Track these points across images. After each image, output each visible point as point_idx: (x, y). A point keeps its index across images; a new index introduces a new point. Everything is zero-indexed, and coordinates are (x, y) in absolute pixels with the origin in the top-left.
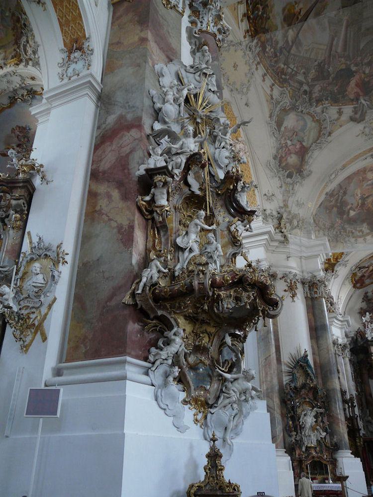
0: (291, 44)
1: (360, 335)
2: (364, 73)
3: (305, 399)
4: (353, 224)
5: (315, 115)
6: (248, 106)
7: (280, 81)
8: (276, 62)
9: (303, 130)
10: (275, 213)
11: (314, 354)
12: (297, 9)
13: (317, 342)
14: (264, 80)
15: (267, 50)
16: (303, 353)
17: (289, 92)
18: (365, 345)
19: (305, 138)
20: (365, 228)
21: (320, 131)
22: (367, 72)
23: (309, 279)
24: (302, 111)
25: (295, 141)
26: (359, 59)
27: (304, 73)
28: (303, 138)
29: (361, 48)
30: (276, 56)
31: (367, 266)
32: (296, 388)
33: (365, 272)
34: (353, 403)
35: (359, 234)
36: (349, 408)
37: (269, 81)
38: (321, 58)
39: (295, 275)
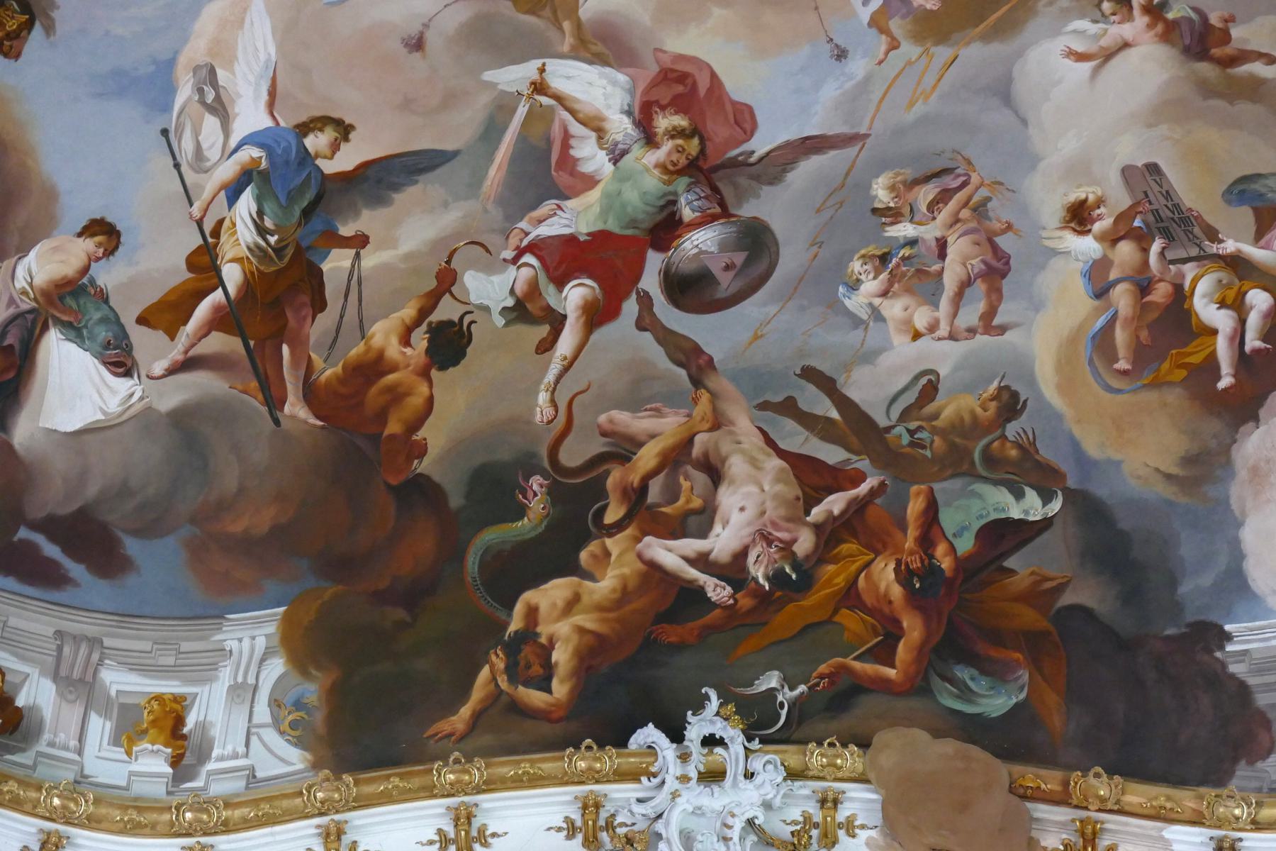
20: (243, 692)
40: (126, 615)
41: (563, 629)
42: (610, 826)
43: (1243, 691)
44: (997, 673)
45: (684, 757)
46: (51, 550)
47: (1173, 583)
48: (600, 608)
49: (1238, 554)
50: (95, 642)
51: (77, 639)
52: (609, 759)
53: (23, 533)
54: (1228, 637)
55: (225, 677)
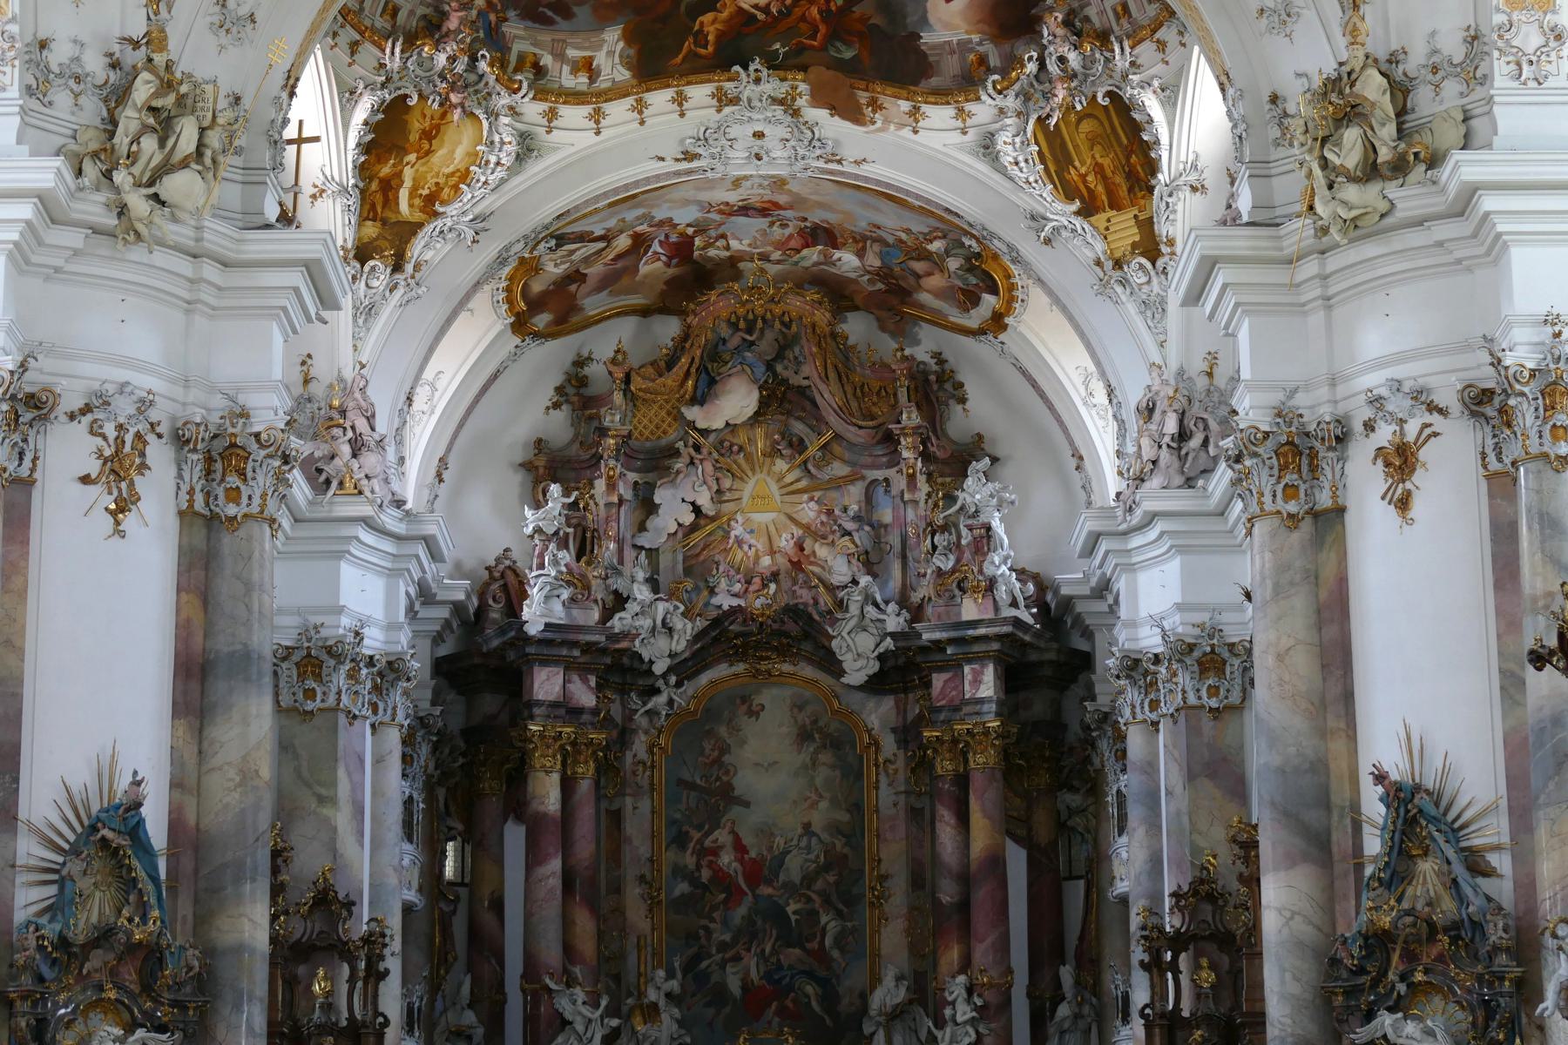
1: (505, 587)
3: (100, 988)
4: (546, 21)
10: (95, 65)
11: (176, 784)
13: (200, 733)
16: (123, 783)
18: (511, 655)
20: (611, 53)
23: (215, 419)
31: (599, 232)
32: (63, 942)
33: (586, 260)
34: (374, 959)
35: (569, 80)
36: (352, 980)
39: (144, 405)
40: (574, 32)
41: (711, 29)
42: (725, 94)
43: (925, 55)
44: (848, 44)
45: (748, 76)
46: (550, 13)
47: (905, 17)
48: (724, 22)
49: (925, 12)
50: (564, 41)
51: (559, 41)
52: (727, 75)
53: (541, 9)
54: (921, 37)
55: (605, 49)
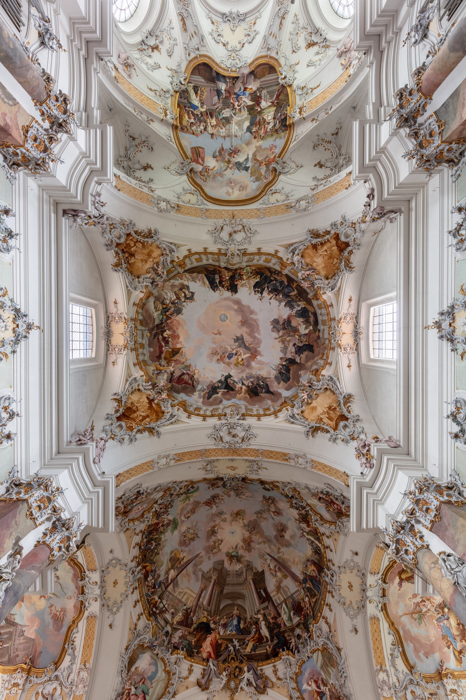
0: (170, 581)
2: (219, 634)
5: (168, 664)
6: (111, 628)
7: (149, 612)
8: (153, 593)
9: (151, 678)
12: (181, 556)
14: (135, 606)
15: (149, 579)
17: (153, 627)
19: (151, 691)
21: (167, 687)
22: (221, 634)
24: (157, 654)
25: (139, 692)
26: (218, 618)
27: (173, 614)
28: (148, 690)
29: (221, 607)
30: (154, 587)
37: (139, 608)
38: (190, 604)
